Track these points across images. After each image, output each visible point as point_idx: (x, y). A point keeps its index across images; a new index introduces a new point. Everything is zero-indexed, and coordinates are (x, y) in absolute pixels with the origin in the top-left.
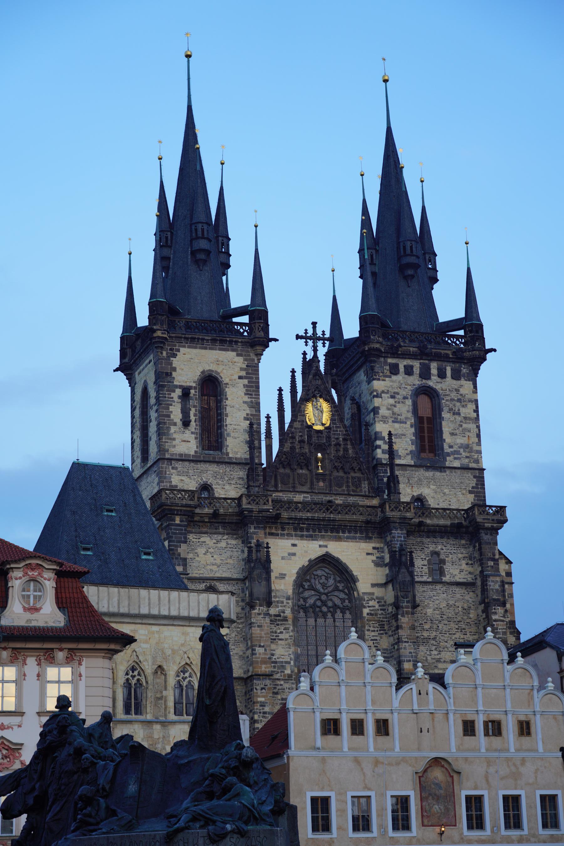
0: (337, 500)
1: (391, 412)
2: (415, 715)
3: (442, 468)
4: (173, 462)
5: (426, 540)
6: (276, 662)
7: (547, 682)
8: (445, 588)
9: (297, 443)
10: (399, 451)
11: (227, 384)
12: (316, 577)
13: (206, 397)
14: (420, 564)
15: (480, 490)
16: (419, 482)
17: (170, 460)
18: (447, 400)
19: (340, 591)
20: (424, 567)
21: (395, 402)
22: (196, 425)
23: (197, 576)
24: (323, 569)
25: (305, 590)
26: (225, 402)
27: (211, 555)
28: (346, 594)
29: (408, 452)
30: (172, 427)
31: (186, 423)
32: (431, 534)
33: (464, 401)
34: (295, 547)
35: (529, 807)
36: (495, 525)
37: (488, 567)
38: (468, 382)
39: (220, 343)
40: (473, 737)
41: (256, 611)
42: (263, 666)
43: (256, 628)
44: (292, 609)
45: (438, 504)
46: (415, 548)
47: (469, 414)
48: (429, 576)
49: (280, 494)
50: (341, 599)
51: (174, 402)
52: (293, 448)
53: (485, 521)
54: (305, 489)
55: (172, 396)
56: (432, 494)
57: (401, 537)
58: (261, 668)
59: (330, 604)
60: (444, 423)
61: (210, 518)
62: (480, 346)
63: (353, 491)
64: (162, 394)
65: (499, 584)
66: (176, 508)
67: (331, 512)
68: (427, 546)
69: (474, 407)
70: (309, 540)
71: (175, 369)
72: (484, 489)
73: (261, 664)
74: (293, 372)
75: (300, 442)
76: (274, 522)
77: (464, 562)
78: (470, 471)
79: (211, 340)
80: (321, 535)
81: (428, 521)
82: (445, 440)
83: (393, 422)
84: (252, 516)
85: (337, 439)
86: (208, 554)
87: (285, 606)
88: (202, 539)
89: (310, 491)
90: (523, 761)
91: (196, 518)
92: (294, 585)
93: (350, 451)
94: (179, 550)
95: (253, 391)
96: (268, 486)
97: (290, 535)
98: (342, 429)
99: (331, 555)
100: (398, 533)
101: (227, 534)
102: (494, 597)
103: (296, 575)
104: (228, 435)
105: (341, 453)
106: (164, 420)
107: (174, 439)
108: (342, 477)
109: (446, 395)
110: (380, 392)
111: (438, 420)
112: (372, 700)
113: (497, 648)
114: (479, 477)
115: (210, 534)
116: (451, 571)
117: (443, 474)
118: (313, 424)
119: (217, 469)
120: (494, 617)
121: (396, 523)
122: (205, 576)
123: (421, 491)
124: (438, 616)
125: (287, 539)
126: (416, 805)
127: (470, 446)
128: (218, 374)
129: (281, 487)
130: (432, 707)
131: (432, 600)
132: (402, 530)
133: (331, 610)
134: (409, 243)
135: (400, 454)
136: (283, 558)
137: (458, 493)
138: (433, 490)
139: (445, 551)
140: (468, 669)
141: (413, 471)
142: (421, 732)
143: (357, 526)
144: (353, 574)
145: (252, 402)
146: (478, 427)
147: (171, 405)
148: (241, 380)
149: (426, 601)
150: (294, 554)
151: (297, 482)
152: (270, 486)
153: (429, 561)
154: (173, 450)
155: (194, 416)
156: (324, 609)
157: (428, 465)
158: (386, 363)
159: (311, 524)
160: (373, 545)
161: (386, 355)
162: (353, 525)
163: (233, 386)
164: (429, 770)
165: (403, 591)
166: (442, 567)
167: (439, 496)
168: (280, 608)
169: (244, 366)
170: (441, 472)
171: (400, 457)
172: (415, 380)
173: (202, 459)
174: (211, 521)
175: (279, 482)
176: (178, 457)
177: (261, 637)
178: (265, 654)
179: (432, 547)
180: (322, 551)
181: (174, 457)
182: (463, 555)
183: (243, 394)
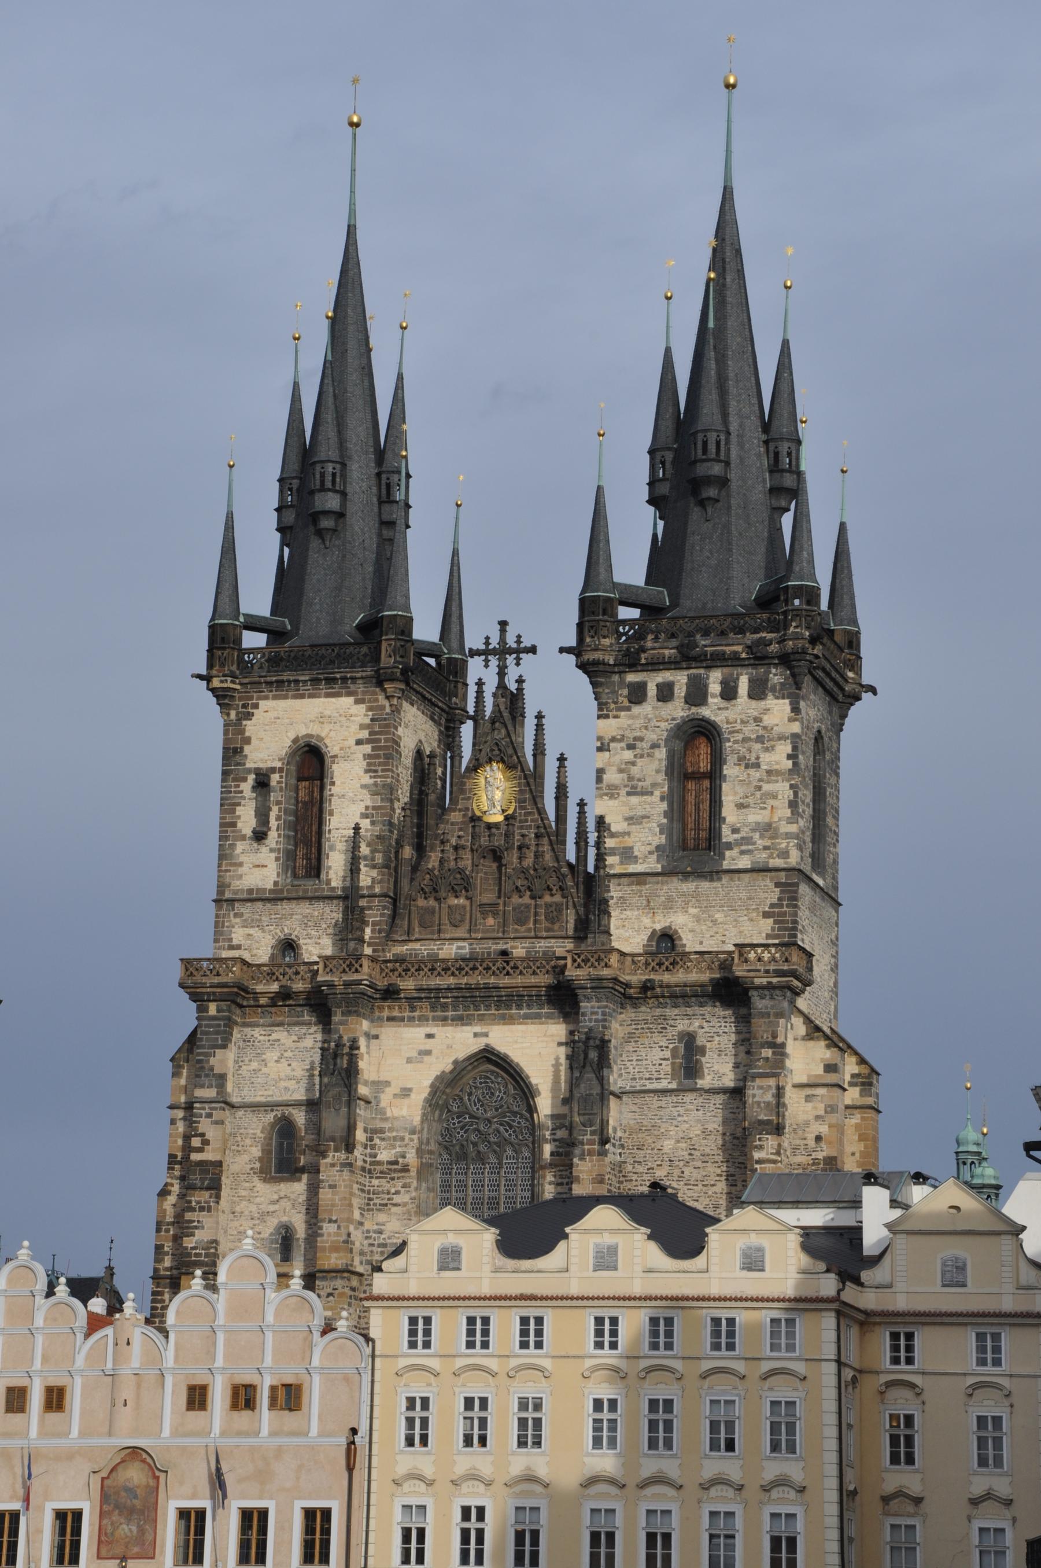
0: (516, 948)
1: (625, 776)
3: (715, 874)
4: (237, 905)
5: (670, 1012)
6: (385, 1245)
8: (701, 1100)
10: (636, 849)
11: (336, 756)
14: (656, 1058)
15: (785, 909)
16: (669, 905)
17: (232, 901)
18: (736, 742)
20: (664, 1063)
21: (635, 756)
22: (279, 836)
23: (263, 1099)
26: (330, 790)
28: (526, 1120)
29: (652, 848)
30: (238, 843)
31: (260, 836)
32: (680, 1000)
34: (431, 1040)
35: (279, 1528)
36: (775, 980)
37: (759, 1060)
38: (781, 701)
40: (203, 1413)
41: (329, 1160)
42: (334, 1255)
43: (327, 1190)
44: (419, 1152)
45: (701, 943)
47: (777, 763)
48: (673, 1079)
49: (417, 946)
51: (244, 798)
52: (442, 861)
53: (752, 974)
54: (461, 932)
56: (690, 925)
57: (596, 1013)
58: (329, 1258)
60: (724, 785)
62: (798, 630)
63: (548, 930)
65: (774, 1091)
66: (204, 990)
68: (672, 1022)
69: (789, 749)
70: (457, 1025)
73: (330, 1252)
75: (456, 848)
78: (769, 874)
81: (667, 978)
82: (724, 819)
83: (629, 794)
85: (523, 836)
87: (406, 1146)
88: (274, 1036)
89: (467, 936)
91: (263, 1001)
92: (424, 1108)
96: (396, 932)
97: (423, 1020)
98: (536, 816)
100: (592, 1007)
102: (760, 1118)
103: (428, 1090)
104: (332, 848)
105: (529, 861)
107: (241, 864)
108: (528, 906)
109: (734, 732)
110: (606, 741)
111: (718, 782)
112: (43, 1355)
115: (289, 1025)
116: (716, 1068)
117: (715, 884)
119: (308, 911)
120: (757, 1155)
121: (587, 988)
122: (275, 1099)
124: (685, 1153)
125: (419, 1026)
126: (91, 1524)
128: (320, 738)
129: (420, 932)
131: (675, 1123)
132: (599, 1000)
134: (715, 434)
135: (636, 853)
136: (409, 1060)
137: (741, 919)
138: (694, 916)
139: (707, 1029)
141: (658, 883)
145: (376, 784)
147: (239, 804)
148: (361, 747)
149: (664, 1125)
150: (428, 1053)
153: (674, 1051)
154: (238, 883)
155: (277, 820)
158: (622, 684)
159: (458, 997)
161: (622, 668)
163: (346, 758)
164: (120, 1469)
165: (584, 1114)
166: (697, 1061)
167: (704, 927)
168: (398, 1149)
169: (367, 721)
170: (712, 880)
171: (635, 859)
172: (677, 710)
173: (285, 894)
175: (417, 924)
176: (245, 896)
177: (333, 1205)
178: (337, 1234)
179: (682, 1025)
181: (239, 896)
183: (362, 773)
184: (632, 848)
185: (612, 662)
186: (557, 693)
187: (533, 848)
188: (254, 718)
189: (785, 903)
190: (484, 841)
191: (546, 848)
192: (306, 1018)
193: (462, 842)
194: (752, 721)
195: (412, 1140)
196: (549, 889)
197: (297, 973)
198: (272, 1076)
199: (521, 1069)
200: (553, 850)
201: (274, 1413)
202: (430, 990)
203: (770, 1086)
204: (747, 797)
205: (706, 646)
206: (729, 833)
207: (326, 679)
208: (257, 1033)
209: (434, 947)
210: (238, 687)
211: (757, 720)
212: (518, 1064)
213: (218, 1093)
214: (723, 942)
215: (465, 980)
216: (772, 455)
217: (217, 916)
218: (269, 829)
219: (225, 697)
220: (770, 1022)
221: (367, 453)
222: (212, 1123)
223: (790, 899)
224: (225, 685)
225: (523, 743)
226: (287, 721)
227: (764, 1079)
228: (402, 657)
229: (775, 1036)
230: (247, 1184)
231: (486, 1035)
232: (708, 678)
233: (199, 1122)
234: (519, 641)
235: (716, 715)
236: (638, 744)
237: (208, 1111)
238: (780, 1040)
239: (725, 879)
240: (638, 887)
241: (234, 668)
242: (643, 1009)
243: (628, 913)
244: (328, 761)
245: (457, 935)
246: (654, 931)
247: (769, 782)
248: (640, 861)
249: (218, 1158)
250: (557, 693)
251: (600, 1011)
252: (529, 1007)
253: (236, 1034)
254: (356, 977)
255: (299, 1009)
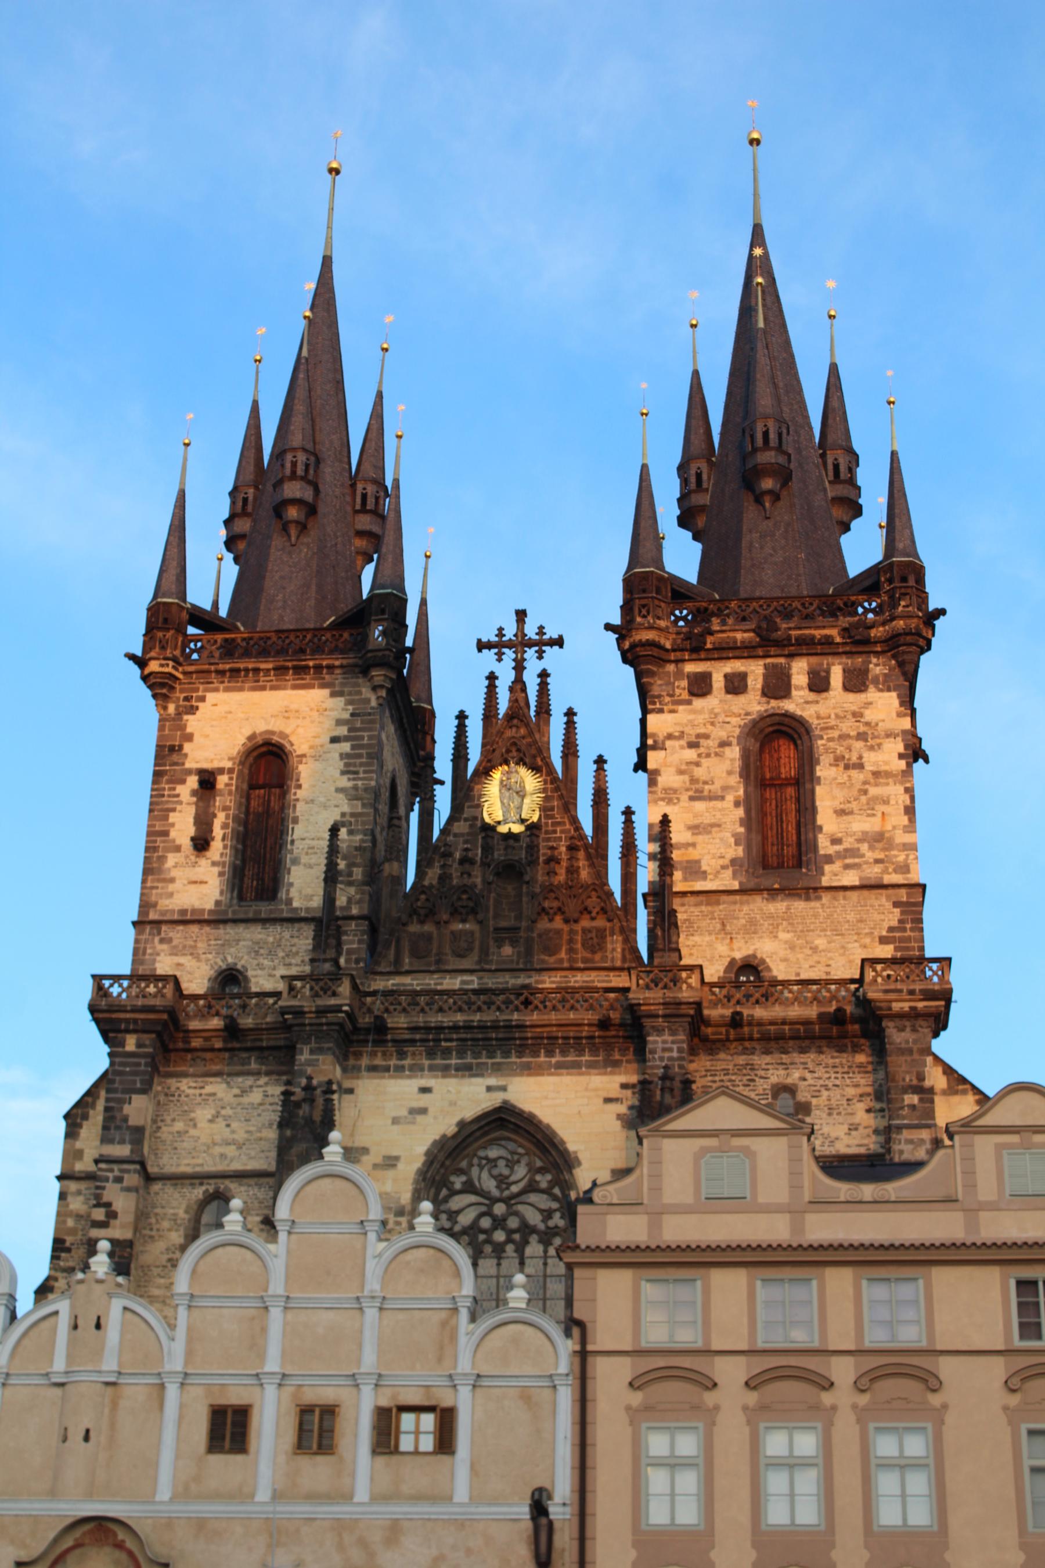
0: (543, 982)
1: (686, 778)
2: (58, 1391)
3: (811, 891)
5: (760, 1060)
7: (510, 1287)
9: (456, 865)
12: (484, 1162)
13: (262, 791)
16: (751, 928)
17: (158, 923)
18: (830, 740)
19: (543, 1191)
21: (699, 755)
22: (225, 847)
23: (189, 1170)
24: (503, 1142)
25: (454, 1193)
26: (295, 794)
27: (224, 1123)
28: (555, 1198)
29: (726, 861)
31: (201, 844)
32: (773, 1044)
33: (874, 737)
34: (427, 1096)
36: (920, 1005)
37: (902, 1108)
38: (886, 694)
39: (294, 674)
40: (239, 1458)
45: (798, 974)
46: (730, 1081)
47: (886, 763)
49: (407, 980)
50: (541, 1211)
51: (181, 803)
52: (443, 878)
53: (892, 996)
54: (466, 964)
55: (177, 792)
56: (782, 953)
57: (671, 1050)
59: (513, 1223)
60: (819, 790)
61: (225, 1041)
62: (910, 609)
64: (156, 790)
65: (928, 1146)
66: (122, 1016)
67: (517, 1009)
68: (762, 1073)
69: (900, 747)
70: (463, 1076)
71: (189, 738)
72: (922, 930)
74: (462, 717)
75: (463, 861)
76: (366, 1038)
77: (860, 1108)
78: (884, 892)
79: (274, 669)
80: (493, 1064)
81: (760, 1013)
82: (820, 828)
84: (304, 1025)
85: (552, 848)
86: (220, 1119)
88: (209, 1089)
90: (394, 1531)
91: (196, 1043)
92: (416, 1182)
93: (584, 874)
94: (127, 1109)
95: (361, 765)
96: (378, 963)
97: (416, 1070)
98: (568, 826)
99: (514, 1107)
101: (268, 1073)
103: (422, 1159)
104: (295, 861)
105: (561, 877)
106: (156, 841)
107: (172, 880)
108: (559, 932)
109: (827, 728)
110: (661, 738)
113: (354, 1191)
114: (908, 904)
115: (229, 1075)
116: (826, 1130)
117: (813, 904)
118: (499, 823)
119: (260, 936)
121: (657, 1016)
123: (752, 948)
125: (410, 1077)
127: (887, 835)
128: (287, 736)
129: (411, 964)
130: (110, 1364)
132: (673, 1033)
133: (517, 1237)
135: (704, 868)
136: (395, 1121)
137: (850, 946)
139: (811, 1082)
140: (249, 1255)
141: (735, 903)
142: (65, 1439)
143: (581, 1038)
144: (566, 1150)
145: (355, 788)
146: (910, 791)
147: (174, 810)
148: (336, 746)
150: (423, 1111)
151: (448, 950)
152: (383, 964)
154: (167, 902)
156: (500, 1236)
157: (776, 886)
159: (466, 1040)
160: (623, 1079)
162: (572, 1034)
164: (71, 1558)
167: (800, 956)
169: (346, 716)
170: (808, 899)
171: (704, 875)
172: (752, 704)
173: (230, 916)
174: (230, 1046)
176: (176, 917)
179: (776, 1076)
180: (495, 1100)
181: (168, 917)
182: (860, 1091)
184: (698, 862)
185: (668, 646)
186: (593, 689)
187: (564, 864)
188: (198, 713)
189: (908, 926)
190: (499, 855)
191: (582, 863)
192: (254, 1066)
193: (470, 854)
194: (849, 716)
195: (398, 1223)
196: (586, 910)
197: (244, 1006)
198: (203, 1140)
199: (554, 1133)
200: (592, 865)
201: (381, 1460)
202: (428, 1029)
203: (922, 1141)
204: (849, 802)
205: (790, 629)
206: (828, 844)
207: (295, 668)
208: (186, 1085)
209: (431, 982)
210: (181, 676)
211: (857, 715)
212: (548, 1126)
213: (132, 1151)
214: (828, 973)
215: (477, 1017)
216: (830, 467)
217: (137, 941)
218: (213, 839)
219: (163, 685)
220: (913, 1060)
221: (341, 461)
222: (123, 1189)
223: (913, 921)
224: (166, 670)
225: (548, 743)
226: (242, 716)
227: (913, 1131)
228: (394, 640)
229: (921, 1078)
230: (162, 1281)
231: (504, 1089)
232: (790, 668)
233: (103, 1188)
234: (541, 631)
235: (803, 710)
236: (702, 742)
237: (117, 1173)
238: (927, 1083)
239: (826, 898)
240: (709, 908)
241: (177, 653)
242: (722, 1056)
243: (697, 938)
244: (293, 761)
245: (462, 967)
246: (733, 961)
247: (876, 785)
248: (709, 877)
249: (128, 1235)
250: (593, 689)
251: (675, 1047)
252: (564, 1053)
253: (157, 1088)
254: (333, 1001)
255: (244, 1055)
